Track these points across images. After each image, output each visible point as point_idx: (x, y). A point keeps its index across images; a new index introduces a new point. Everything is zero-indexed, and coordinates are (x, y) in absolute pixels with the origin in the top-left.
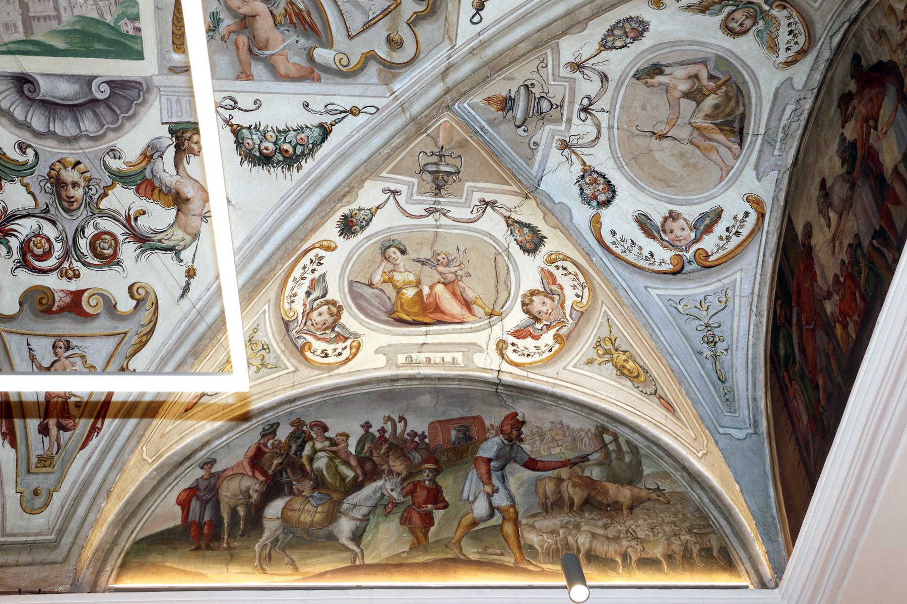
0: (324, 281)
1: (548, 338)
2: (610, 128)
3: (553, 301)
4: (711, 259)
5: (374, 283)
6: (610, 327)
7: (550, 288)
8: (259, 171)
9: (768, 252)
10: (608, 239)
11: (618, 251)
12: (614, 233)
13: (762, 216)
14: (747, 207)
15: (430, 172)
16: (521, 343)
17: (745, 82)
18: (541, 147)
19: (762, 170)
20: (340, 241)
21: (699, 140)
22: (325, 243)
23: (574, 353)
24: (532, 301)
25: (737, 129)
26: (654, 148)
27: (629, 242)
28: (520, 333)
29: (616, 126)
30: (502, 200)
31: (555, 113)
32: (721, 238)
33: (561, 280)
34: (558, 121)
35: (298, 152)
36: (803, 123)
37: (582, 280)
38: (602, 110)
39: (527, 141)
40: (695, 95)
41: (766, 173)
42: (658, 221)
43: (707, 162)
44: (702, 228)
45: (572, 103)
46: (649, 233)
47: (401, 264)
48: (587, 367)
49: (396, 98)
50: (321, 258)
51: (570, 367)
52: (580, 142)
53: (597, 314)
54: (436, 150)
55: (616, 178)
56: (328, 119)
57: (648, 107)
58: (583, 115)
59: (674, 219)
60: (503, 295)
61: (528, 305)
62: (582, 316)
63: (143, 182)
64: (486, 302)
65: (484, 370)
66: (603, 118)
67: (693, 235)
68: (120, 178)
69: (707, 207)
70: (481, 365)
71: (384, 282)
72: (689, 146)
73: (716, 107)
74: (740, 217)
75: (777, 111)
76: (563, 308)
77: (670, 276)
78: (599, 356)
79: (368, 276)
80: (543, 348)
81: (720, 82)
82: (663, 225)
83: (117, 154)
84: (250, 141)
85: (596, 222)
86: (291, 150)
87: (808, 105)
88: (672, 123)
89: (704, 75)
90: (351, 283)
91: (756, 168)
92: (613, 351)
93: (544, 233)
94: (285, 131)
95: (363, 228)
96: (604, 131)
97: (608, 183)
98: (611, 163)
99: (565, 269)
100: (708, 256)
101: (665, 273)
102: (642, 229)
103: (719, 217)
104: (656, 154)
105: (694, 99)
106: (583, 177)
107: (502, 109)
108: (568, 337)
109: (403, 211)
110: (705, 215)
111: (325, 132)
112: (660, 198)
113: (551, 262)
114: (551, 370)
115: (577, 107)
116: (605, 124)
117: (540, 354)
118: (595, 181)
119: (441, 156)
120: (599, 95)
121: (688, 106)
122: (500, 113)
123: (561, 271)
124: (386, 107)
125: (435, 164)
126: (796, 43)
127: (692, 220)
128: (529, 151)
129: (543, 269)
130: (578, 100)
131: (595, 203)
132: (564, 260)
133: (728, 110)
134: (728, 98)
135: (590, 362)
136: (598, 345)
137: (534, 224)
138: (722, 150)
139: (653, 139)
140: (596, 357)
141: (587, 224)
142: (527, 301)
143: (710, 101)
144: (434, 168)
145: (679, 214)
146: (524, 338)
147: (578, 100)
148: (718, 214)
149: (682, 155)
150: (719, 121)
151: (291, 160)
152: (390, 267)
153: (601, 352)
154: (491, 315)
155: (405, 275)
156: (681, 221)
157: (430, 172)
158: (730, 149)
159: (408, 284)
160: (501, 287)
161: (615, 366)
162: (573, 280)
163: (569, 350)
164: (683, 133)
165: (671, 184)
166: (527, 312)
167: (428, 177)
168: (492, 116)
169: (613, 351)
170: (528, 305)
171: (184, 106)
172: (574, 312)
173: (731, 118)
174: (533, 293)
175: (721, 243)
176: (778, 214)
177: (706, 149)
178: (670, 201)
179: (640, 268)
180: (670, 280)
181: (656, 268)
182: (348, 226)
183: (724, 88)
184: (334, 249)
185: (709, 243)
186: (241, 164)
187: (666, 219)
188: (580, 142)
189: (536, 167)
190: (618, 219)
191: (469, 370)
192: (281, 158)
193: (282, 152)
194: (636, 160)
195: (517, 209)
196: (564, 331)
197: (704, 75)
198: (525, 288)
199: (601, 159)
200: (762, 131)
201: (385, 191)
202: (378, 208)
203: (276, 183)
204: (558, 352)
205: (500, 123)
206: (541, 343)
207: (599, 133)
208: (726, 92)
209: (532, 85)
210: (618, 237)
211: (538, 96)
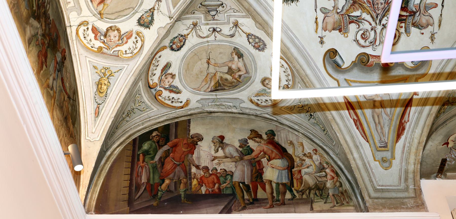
1: (98, 44)
2: (208, 42)
3: (118, 41)
7: (124, 37)
12: (160, 57)
13: (182, 107)
16: (90, 31)
17: (240, 88)
18: (193, 15)
21: (210, 76)
24: (114, 31)
26: (202, 61)
27: (157, 64)
28: (95, 30)
29: (209, 44)
31: (210, 18)
32: (169, 97)
33: (131, 41)
34: (206, 19)
38: (216, 37)
39: (195, 9)
40: (230, 71)
42: (170, 71)
44: (171, 89)
45: (217, 24)
46: (163, 70)
52: (198, 31)
55: (184, 50)
57: (221, 55)
58: (211, 29)
59: (172, 77)
61: (111, 29)
65: (69, 19)
66: (212, 38)
69: (180, 87)
70: (71, 17)
74: (179, 100)
81: (238, 79)
82: (168, 74)
85: (164, 48)
88: (216, 65)
89: (240, 73)
93: (151, 27)
96: (205, 40)
97: (182, 47)
99: (137, 41)
102: (164, 67)
103: (177, 93)
104: (200, 62)
105: (228, 71)
106: (182, 36)
110: (177, 88)
112: (180, 69)
113: (138, 34)
115: (215, 26)
116: (209, 39)
118: (181, 41)
121: (226, 69)
123: (135, 40)
126: (262, 102)
127: (174, 84)
128: (191, 11)
129: (132, 31)
130: (218, 26)
131: (171, 44)
132: (141, 40)
133: (226, 84)
134: (231, 83)
137: (155, 22)
139: (207, 60)
142: (113, 28)
143: (229, 77)
145: (175, 78)
146: (93, 32)
147: (218, 26)
148: (179, 92)
149: (201, 72)
150: (220, 82)
156: (172, 80)
164: (212, 70)
165: (187, 72)
166: (107, 30)
170: (111, 29)
174: (118, 30)
178: (179, 73)
183: (236, 81)
187: (171, 74)
188: (198, 31)
191: (65, 11)
194: (195, 54)
195: (160, 12)
197: (240, 73)
199: (192, 41)
206: (94, 41)
207: (204, 38)
208: (234, 82)
210: (159, 59)
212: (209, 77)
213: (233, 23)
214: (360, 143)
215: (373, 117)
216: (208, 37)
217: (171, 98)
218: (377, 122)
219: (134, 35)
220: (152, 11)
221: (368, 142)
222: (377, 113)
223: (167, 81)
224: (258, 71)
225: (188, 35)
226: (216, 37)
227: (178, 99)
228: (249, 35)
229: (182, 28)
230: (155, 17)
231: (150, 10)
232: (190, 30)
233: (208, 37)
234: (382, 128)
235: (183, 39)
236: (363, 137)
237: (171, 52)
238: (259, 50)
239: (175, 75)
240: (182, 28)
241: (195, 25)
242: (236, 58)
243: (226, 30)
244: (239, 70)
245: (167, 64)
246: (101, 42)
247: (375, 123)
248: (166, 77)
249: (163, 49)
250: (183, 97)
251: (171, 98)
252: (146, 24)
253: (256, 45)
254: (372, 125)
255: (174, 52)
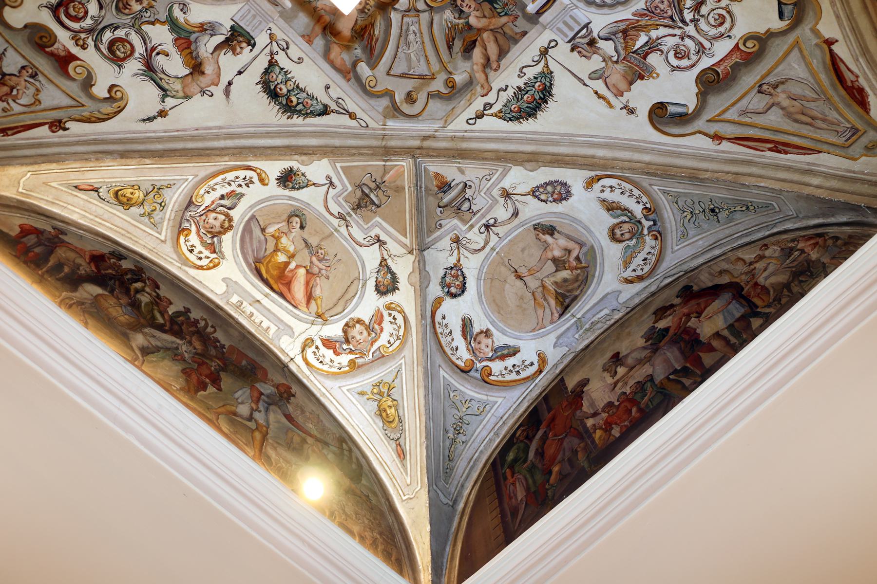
0: (239, 199)
1: (344, 359)
2: (493, 249)
3: (369, 335)
4: (491, 378)
5: (267, 231)
6: (396, 377)
8: (264, 98)
9: (528, 397)
10: (438, 318)
11: (439, 330)
13: (540, 371)
14: (535, 359)
15: (362, 191)
16: (323, 350)
18: (442, 230)
19: (561, 341)
20: (273, 182)
21: (539, 295)
22: (263, 175)
23: (355, 380)
24: (354, 326)
25: (566, 304)
26: (508, 281)
28: (328, 343)
30: (392, 245)
31: (467, 215)
32: (506, 369)
34: (465, 222)
35: (298, 108)
36: (606, 327)
37: (401, 332)
38: (497, 234)
41: (561, 345)
42: (476, 330)
43: (533, 312)
45: (483, 216)
46: (464, 334)
47: (294, 234)
48: (357, 396)
49: (384, 129)
50: (252, 182)
51: (344, 389)
52: (468, 245)
53: (394, 363)
54: (379, 180)
55: (471, 284)
56: (333, 106)
59: (487, 336)
60: (339, 308)
62: (382, 357)
63: (185, 40)
64: (323, 305)
65: (283, 351)
67: (490, 355)
68: (173, 24)
70: (283, 346)
71: (273, 236)
72: (530, 295)
73: (565, 280)
74: (526, 363)
75: (597, 309)
76: (372, 345)
77: (459, 371)
78: (372, 393)
79: (267, 222)
80: (336, 364)
82: (477, 335)
83: (185, 9)
84: (275, 76)
85: (438, 302)
86: (295, 103)
87: (617, 316)
90: (253, 217)
91: (558, 338)
92: (385, 395)
93: (399, 286)
94: (301, 90)
95: (293, 188)
96: (488, 249)
97: (464, 283)
98: (476, 272)
99: (394, 319)
100: (490, 374)
101: (457, 366)
103: (515, 354)
104: (507, 286)
106: (452, 268)
107: (440, 188)
108: (359, 367)
109: (326, 201)
110: (507, 347)
111: (325, 111)
112: (487, 316)
113: (388, 308)
114: (329, 383)
115: (484, 221)
116: (491, 244)
117: (331, 367)
118: (457, 277)
119: (378, 187)
120: (503, 223)
122: (436, 189)
123: (391, 319)
124: (373, 129)
125: (371, 189)
127: (497, 344)
128: (434, 226)
129: (379, 310)
130: (488, 217)
131: (446, 290)
132: (399, 312)
135: (362, 394)
136: (378, 385)
137: (398, 275)
138: (548, 311)
139: (513, 274)
140: (369, 392)
141: (433, 299)
144: (367, 191)
145: (492, 335)
146: (328, 348)
147: (488, 217)
148: (515, 352)
149: (522, 298)
151: (289, 109)
152: (285, 229)
153: (375, 391)
154: (319, 316)
155: (290, 243)
156: (490, 341)
157: (362, 191)
158: (552, 314)
159: (285, 251)
160: (342, 303)
161: (379, 407)
162: (395, 329)
163: (354, 376)
166: (345, 332)
167: (359, 193)
168: (430, 186)
169: (385, 395)
171: (255, 22)
172: (378, 352)
173: (568, 294)
174: (359, 321)
175: (504, 372)
176: (550, 377)
177: (539, 304)
178: (492, 323)
179: (444, 352)
180: (457, 373)
181: (454, 359)
182: (287, 179)
184: (264, 185)
185: (497, 367)
186: (257, 84)
187: (482, 332)
188: (468, 245)
189: (430, 239)
190: (453, 312)
192: (284, 102)
193: (288, 99)
194: (492, 281)
195: (395, 258)
196: (360, 361)
198: (356, 315)
199: (472, 266)
200: (578, 316)
201: (328, 177)
202: (314, 184)
203: (268, 113)
204: (345, 372)
205: (432, 195)
206: (337, 359)
207: (484, 247)
209: (470, 186)
210: (445, 322)
211: (467, 196)
212: (539, 297)
213: (501, 196)
214: (808, 164)
215: (796, 121)
216: (487, 243)
217: (510, 368)
218: (809, 120)
219: (385, 313)
220: (383, 264)
221: (819, 152)
222: (797, 113)
223: (483, 346)
224: (592, 229)
225: (459, 261)
226: (497, 234)
227: (523, 362)
228: (534, 192)
229: (441, 257)
230: (394, 268)
231: (380, 265)
232: (456, 252)
233: (487, 243)
234: (824, 120)
235: (456, 270)
236: (805, 154)
237: (454, 301)
238: (566, 199)
239: (488, 330)
240: (441, 257)
241: (457, 240)
242: (548, 238)
243: (502, 213)
244: (570, 252)
245: (464, 321)
246: (347, 354)
247: (807, 124)
248: (477, 341)
249: (440, 304)
250: (528, 352)
251: (510, 368)
252: (390, 288)
253: (555, 196)
254: (805, 130)
255: (459, 299)
